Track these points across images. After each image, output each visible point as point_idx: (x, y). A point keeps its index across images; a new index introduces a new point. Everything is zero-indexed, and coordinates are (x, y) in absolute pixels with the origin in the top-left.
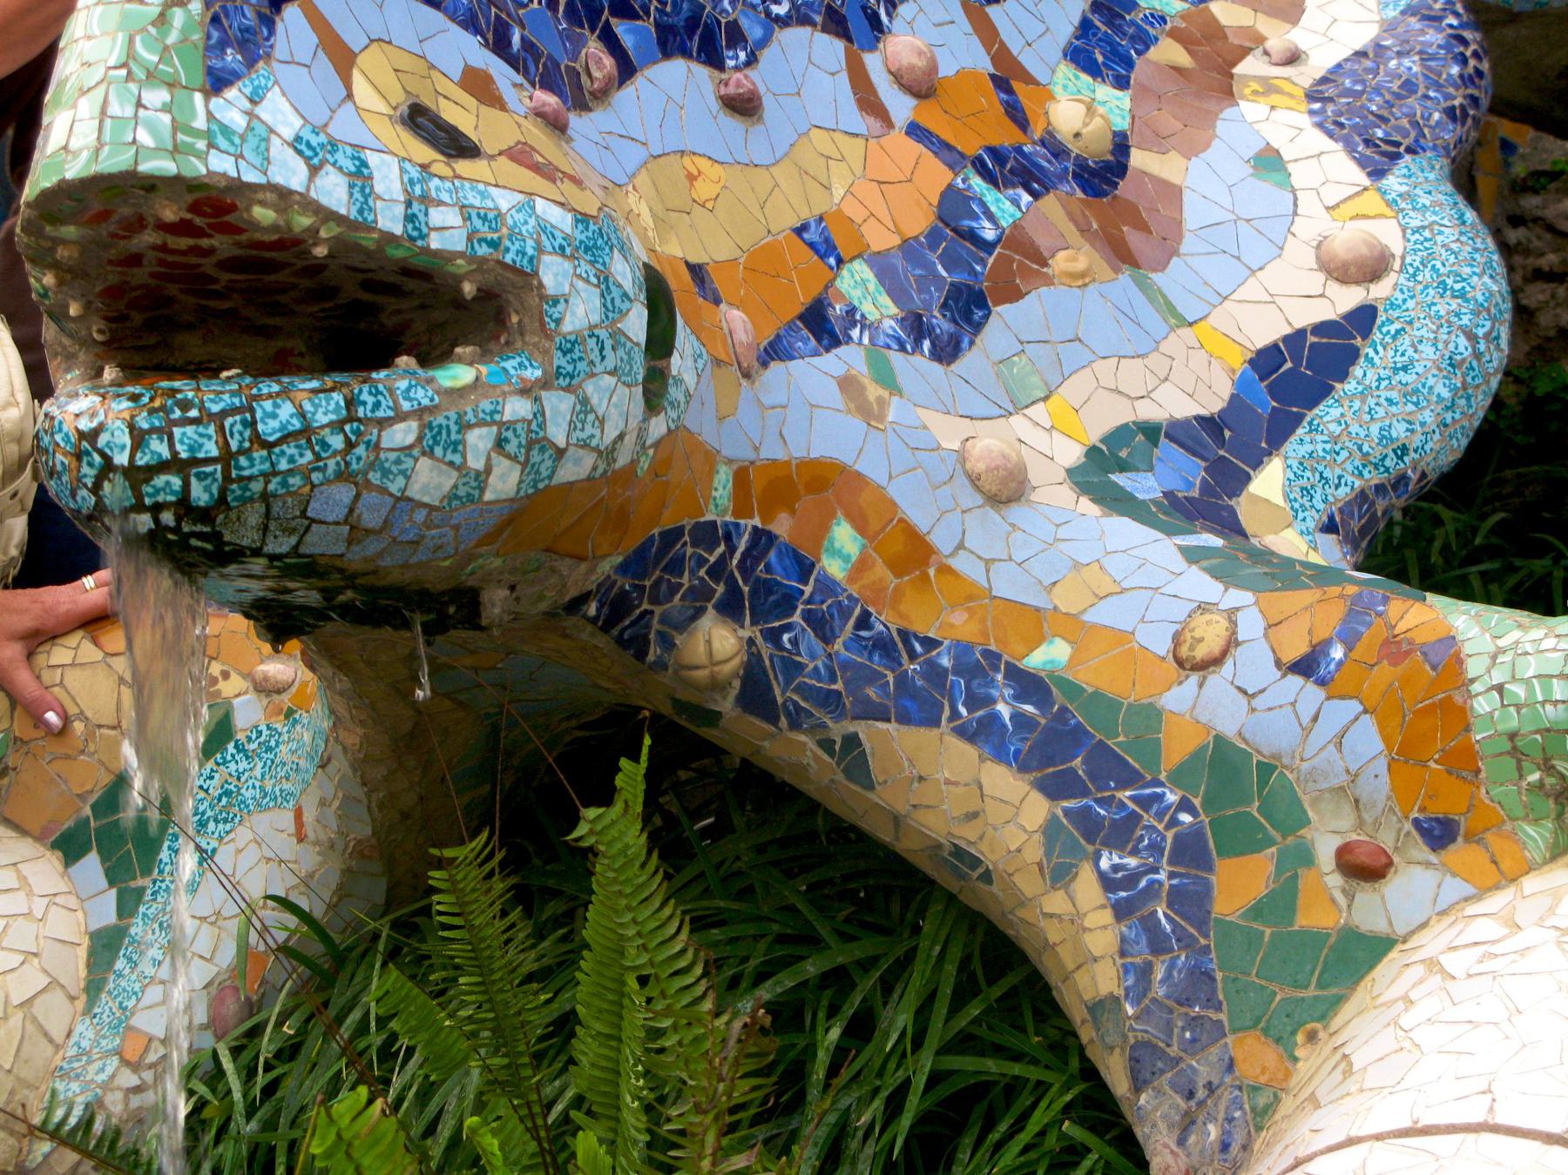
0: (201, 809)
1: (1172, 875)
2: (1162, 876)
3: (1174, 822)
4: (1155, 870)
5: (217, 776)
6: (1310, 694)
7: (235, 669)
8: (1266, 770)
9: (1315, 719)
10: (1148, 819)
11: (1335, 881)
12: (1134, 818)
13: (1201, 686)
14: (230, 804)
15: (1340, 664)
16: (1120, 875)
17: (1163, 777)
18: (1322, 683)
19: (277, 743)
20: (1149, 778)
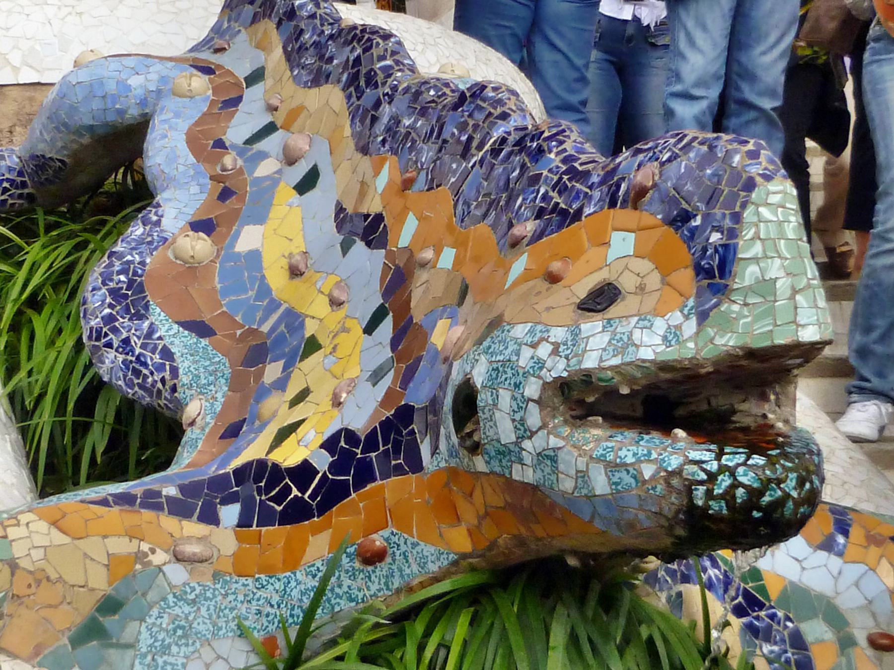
0: (160, 637)
1: (793, 654)
2: (789, 655)
3: (786, 627)
4: (786, 652)
5: (166, 616)
6: (835, 562)
7: (159, 547)
8: (821, 597)
9: (840, 573)
10: (775, 626)
11: (870, 652)
12: (770, 627)
13: (773, 555)
14: (185, 636)
15: (845, 546)
16: (772, 655)
17: (772, 604)
18: (840, 554)
19: (214, 596)
20: (767, 604)
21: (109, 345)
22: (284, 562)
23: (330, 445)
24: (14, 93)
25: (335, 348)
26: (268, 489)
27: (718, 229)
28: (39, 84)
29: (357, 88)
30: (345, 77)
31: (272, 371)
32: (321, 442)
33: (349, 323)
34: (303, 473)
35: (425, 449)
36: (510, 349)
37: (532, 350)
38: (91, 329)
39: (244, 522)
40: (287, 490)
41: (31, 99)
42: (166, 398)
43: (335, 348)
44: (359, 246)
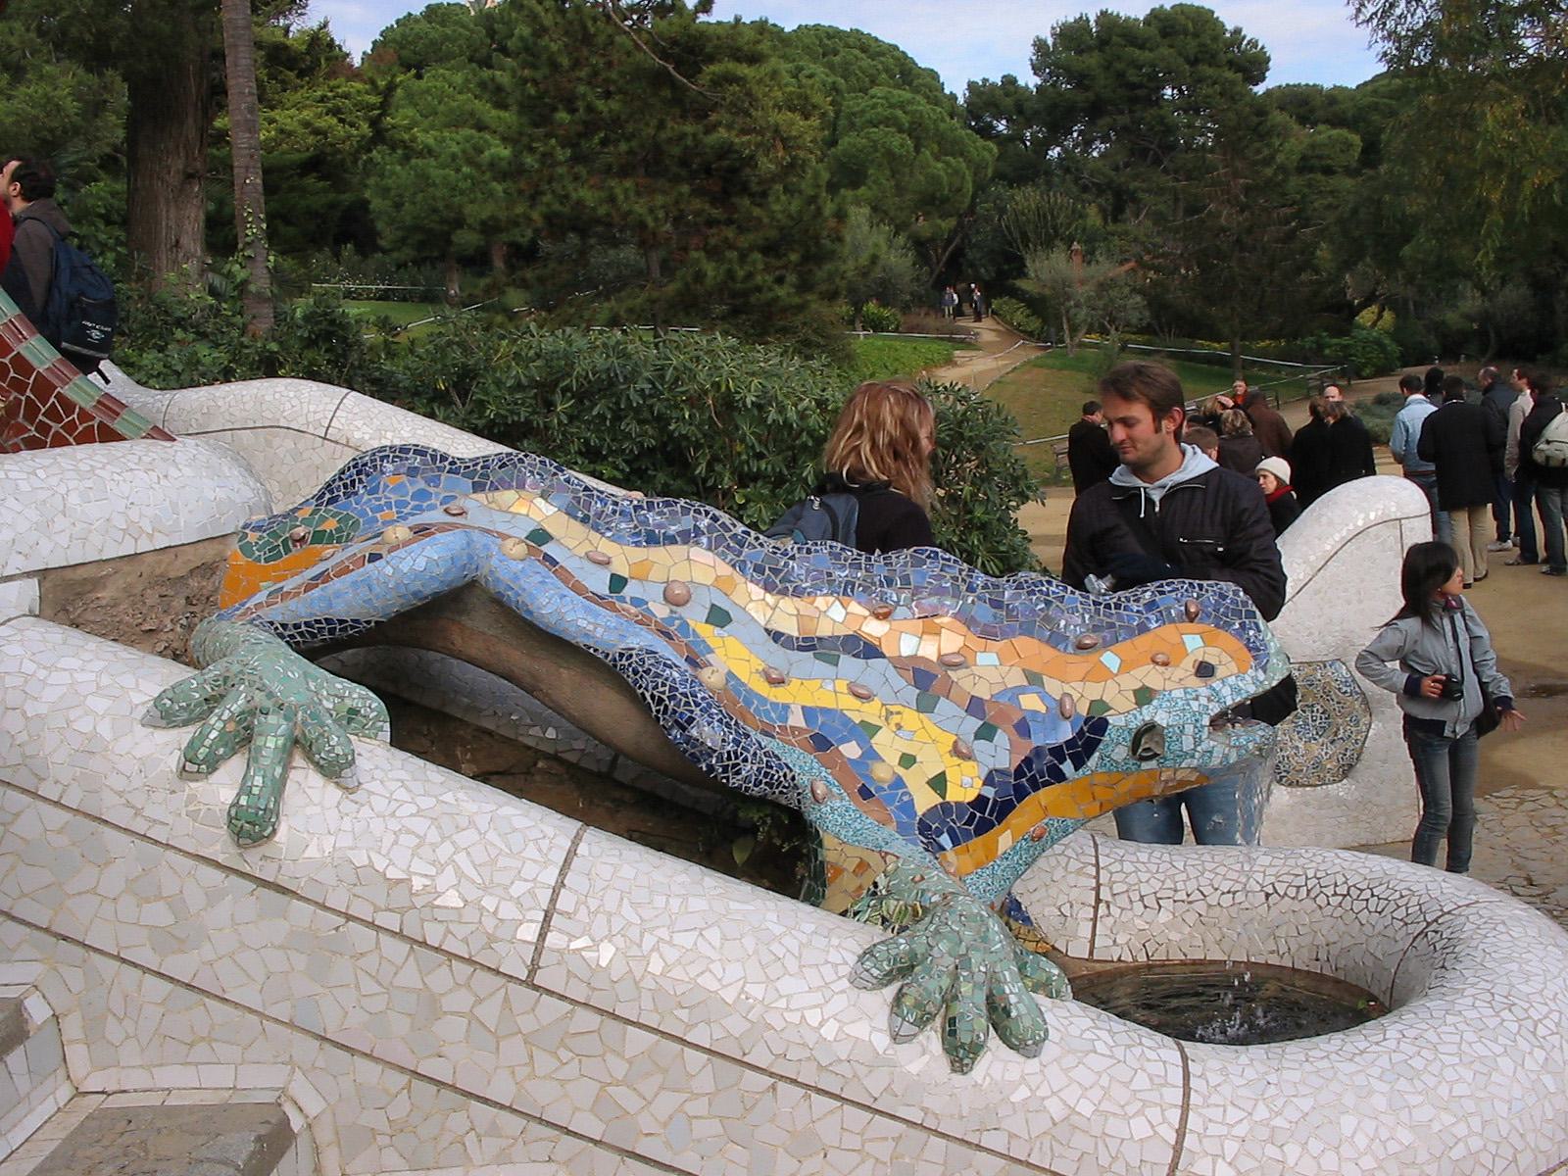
21: (745, 760)
22: (987, 858)
23: (989, 781)
24: (149, 559)
25: (899, 727)
26: (960, 820)
27: (1251, 629)
28: (170, 547)
29: (728, 547)
30: (704, 540)
31: (851, 750)
32: (981, 782)
33: (893, 709)
34: (980, 802)
35: (1067, 767)
36: (1180, 703)
37: (1197, 703)
38: (729, 752)
39: (955, 842)
40: (973, 815)
41: (160, 562)
42: (784, 787)
43: (899, 727)
44: (845, 660)
